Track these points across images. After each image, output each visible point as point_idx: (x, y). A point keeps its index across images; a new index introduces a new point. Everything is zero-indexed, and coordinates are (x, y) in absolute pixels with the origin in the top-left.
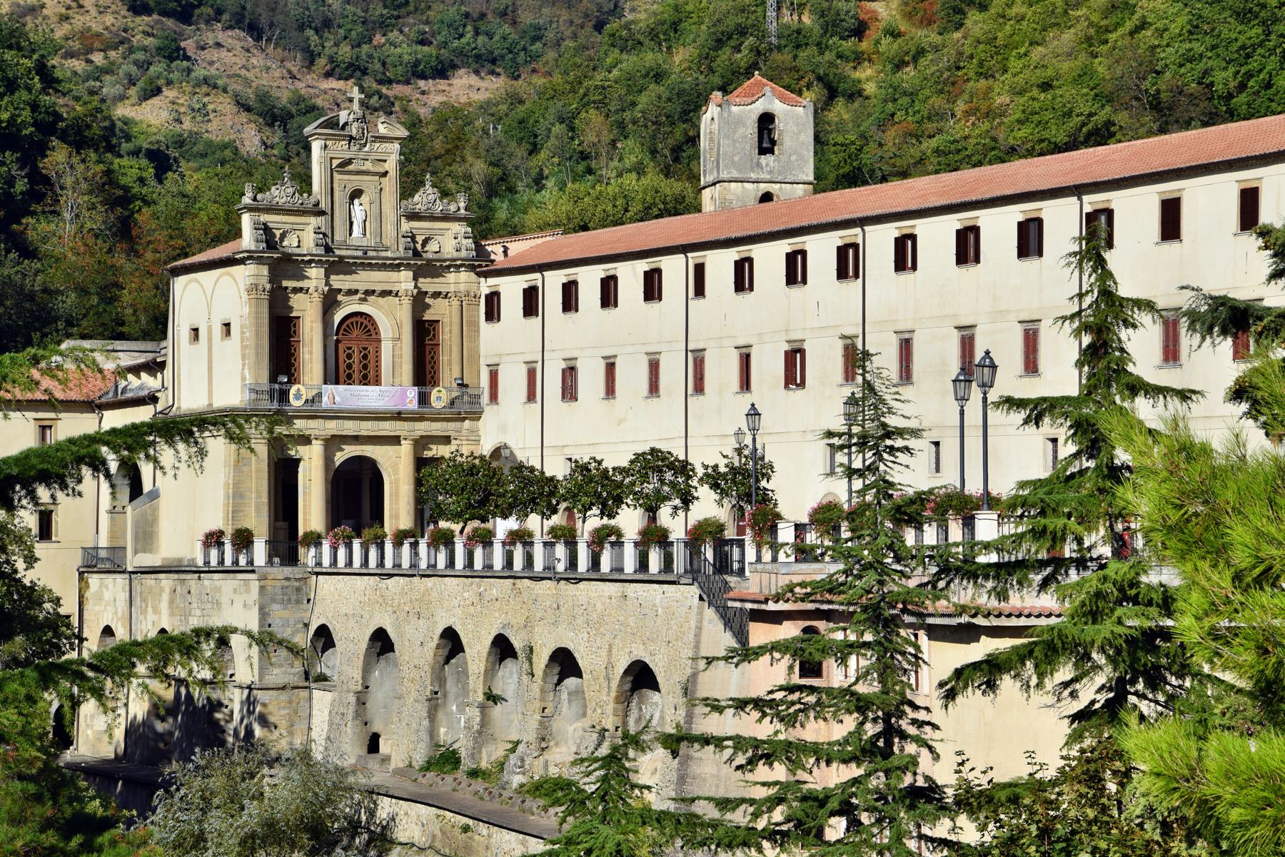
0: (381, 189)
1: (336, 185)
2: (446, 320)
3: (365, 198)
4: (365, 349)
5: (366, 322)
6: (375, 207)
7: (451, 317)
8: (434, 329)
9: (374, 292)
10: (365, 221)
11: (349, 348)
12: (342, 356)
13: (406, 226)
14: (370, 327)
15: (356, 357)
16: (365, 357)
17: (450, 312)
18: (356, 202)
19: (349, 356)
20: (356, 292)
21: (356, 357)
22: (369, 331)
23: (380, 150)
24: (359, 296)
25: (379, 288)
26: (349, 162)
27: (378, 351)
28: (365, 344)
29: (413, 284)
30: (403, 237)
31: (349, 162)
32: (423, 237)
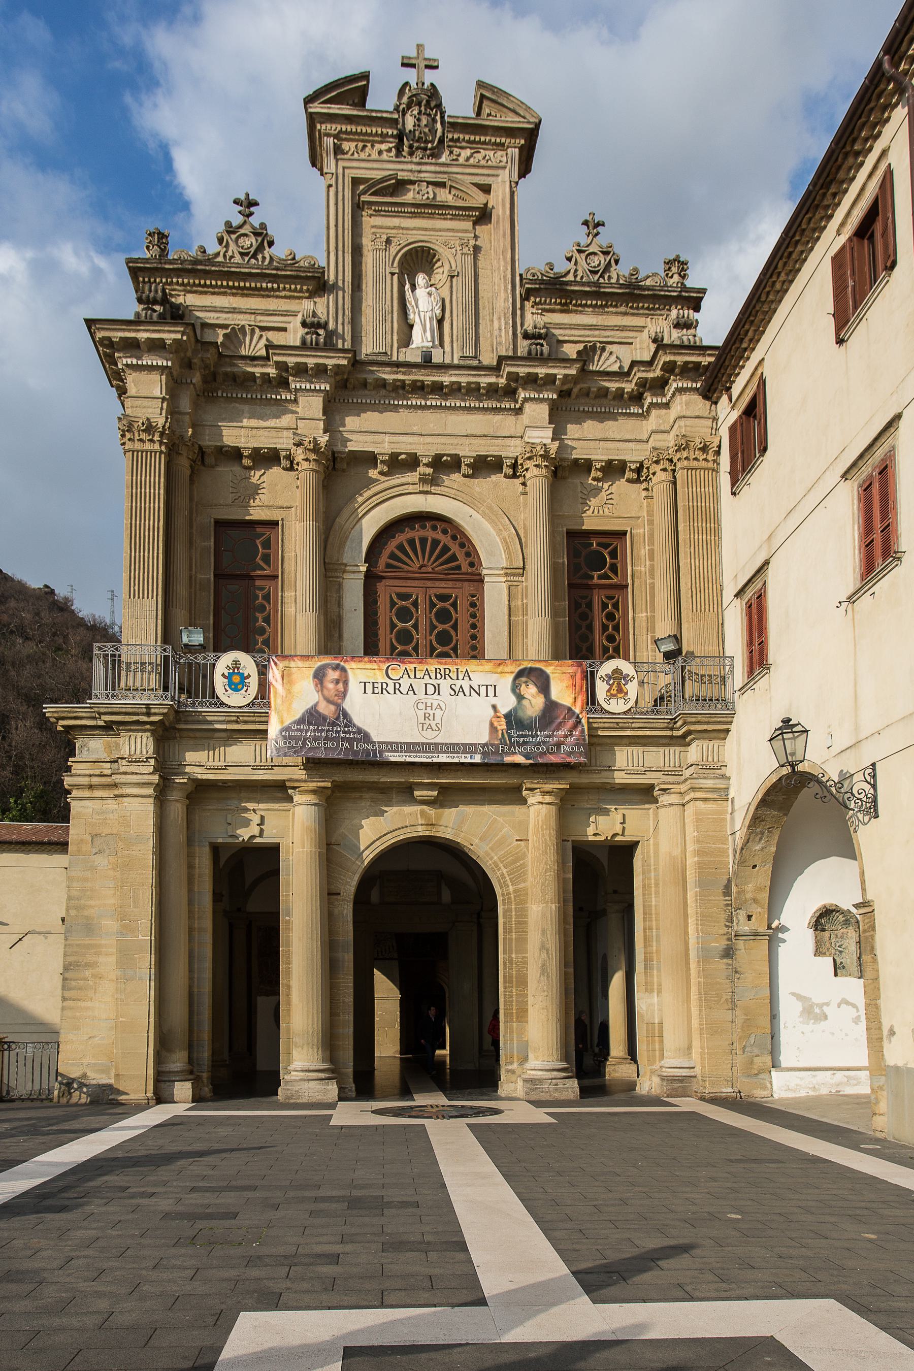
0: (477, 249)
1: (366, 241)
2: (640, 531)
3: (441, 274)
4: (443, 598)
5: (445, 540)
6: (462, 292)
7: (651, 522)
8: (613, 554)
9: (455, 464)
10: (440, 322)
11: (404, 597)
12: (385, 615)
13: (533, 319)
14: (454, 548)
15: (422, 615)
16: (444, 616)
17: (650, 513)
18: (421, 279)
19: (404, 614)
20: (412, 462)
21: (422, 615)
22: (446, 549)
23: (472, 161)
24: (422, 469)
25: (468, 451)
26: (400, 186)
27: (476, 607)
28: (443, 587)
29: (549, 433)
30: (526, 336)
31: (400, 186)
32: (580, 347)
